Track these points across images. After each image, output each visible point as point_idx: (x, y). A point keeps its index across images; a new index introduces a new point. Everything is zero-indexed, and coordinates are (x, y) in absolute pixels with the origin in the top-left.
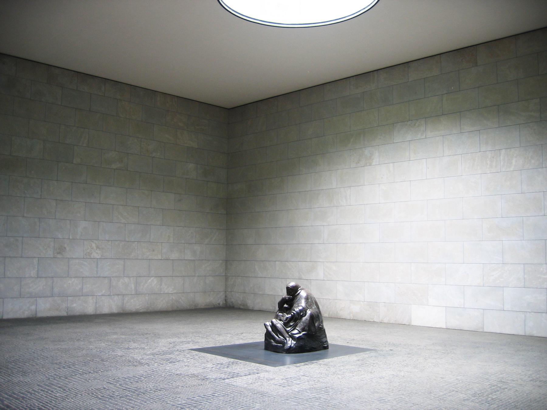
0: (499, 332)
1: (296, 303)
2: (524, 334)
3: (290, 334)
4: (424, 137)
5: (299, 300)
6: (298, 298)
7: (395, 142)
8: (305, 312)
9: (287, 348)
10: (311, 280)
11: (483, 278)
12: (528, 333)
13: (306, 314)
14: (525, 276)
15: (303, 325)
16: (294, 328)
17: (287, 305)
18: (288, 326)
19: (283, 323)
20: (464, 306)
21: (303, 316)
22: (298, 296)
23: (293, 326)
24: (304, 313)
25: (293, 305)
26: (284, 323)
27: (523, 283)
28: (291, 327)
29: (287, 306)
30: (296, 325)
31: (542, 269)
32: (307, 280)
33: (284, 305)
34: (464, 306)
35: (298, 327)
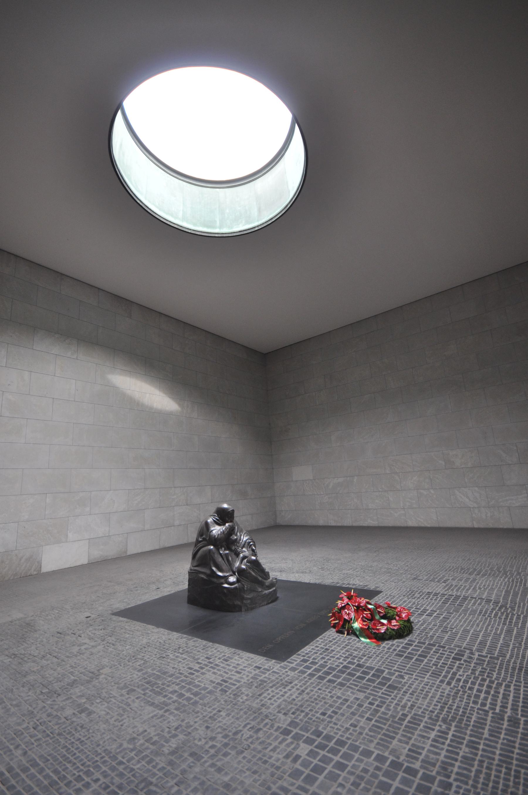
4: (75, 356)
7: (34, 348)
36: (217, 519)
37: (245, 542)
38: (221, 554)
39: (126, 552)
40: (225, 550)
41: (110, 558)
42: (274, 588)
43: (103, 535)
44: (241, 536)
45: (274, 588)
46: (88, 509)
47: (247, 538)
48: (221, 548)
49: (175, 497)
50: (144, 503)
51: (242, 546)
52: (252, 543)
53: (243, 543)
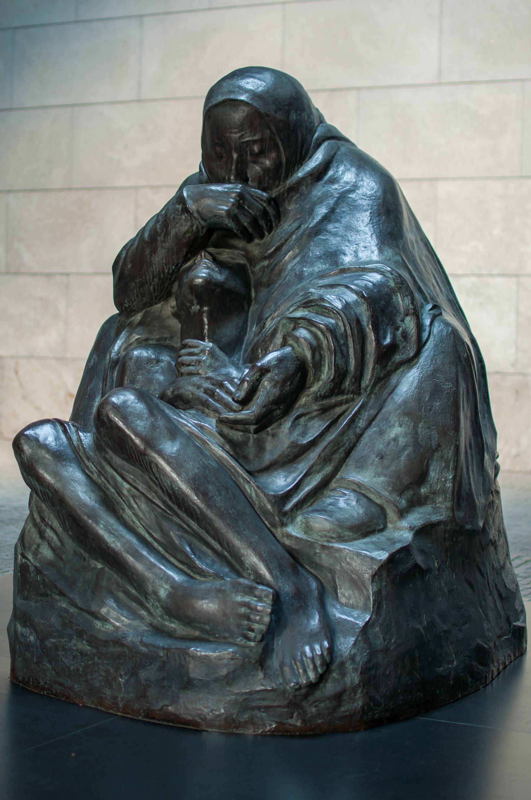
5: (330, 227)
8: (409, 324)
10: (68, 275)
13: (421, 345)
15: (416, 444)
16: (328, 469)
18: (268, 458)
19: (211, 424)
21: (398, 358)
22: (318, 191)
23: (313, 455)
24: (405, 335)
26: (221, 421)
28: (302, 467)
29: (219, 277)
30: (336, 444)
32: (48, 275)
35: (361, 466)
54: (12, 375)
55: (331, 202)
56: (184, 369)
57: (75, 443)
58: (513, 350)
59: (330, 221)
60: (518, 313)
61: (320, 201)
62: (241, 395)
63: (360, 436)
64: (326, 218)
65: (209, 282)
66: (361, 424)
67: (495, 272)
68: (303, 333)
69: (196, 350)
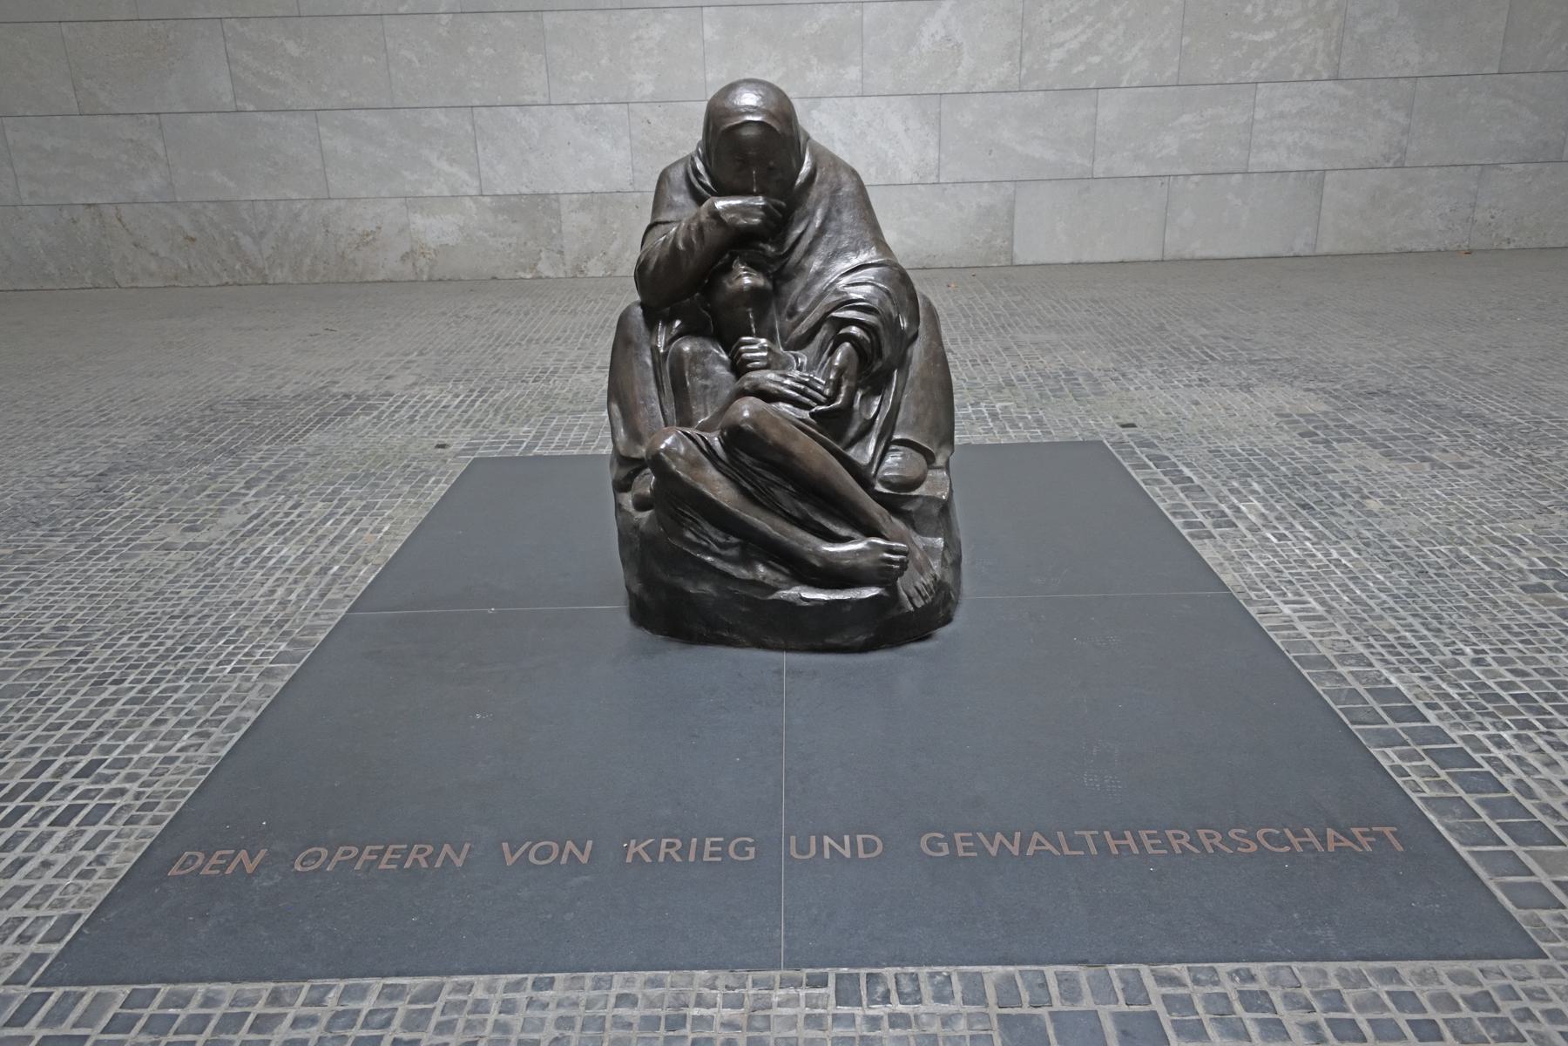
0: (1067, 260)
1: (822, 250)
2: (1158, 257)
3: (879, 488)
6: (819, 213)
9: (920, 603)
11: (1021, 60)
12: (1171, 253)
14: (1186, 40)
17: (755, 266)
20: (938, 176)
25: (799, 269)
27: (1176, 70)
31: (1249, 9)
33: (727, 269)
34: (938, 176)
36: (697, 173)
37: (825, 318)
38: (654, 350)
39: (1009, 252)
40: (682, 334)
41: (944, 264)
42: (869, 593)
43: (916, 180)
44: (820, 274)
45: (869, 593)
46: (853, 73)
47: (856, 293)
48: (668, 322)
49: (1268, 35)
50: (1096, 59)
51: (802, 329)
52: (854, 330)
53: (810, 320)
54: (117, 222)
55: (825, 202)
56: (749, 366)
57: (705, 449)
58: (630, 171)
59: (830, 221)
60: (630, 136)
61: (818, 202)
62: (827, 392)
63: (900, 403)
64: (827, 218)
65: (754, 290)
66: (899, 392)
67: (606, 100)
68: (854, 330)
69: (755, 347)
